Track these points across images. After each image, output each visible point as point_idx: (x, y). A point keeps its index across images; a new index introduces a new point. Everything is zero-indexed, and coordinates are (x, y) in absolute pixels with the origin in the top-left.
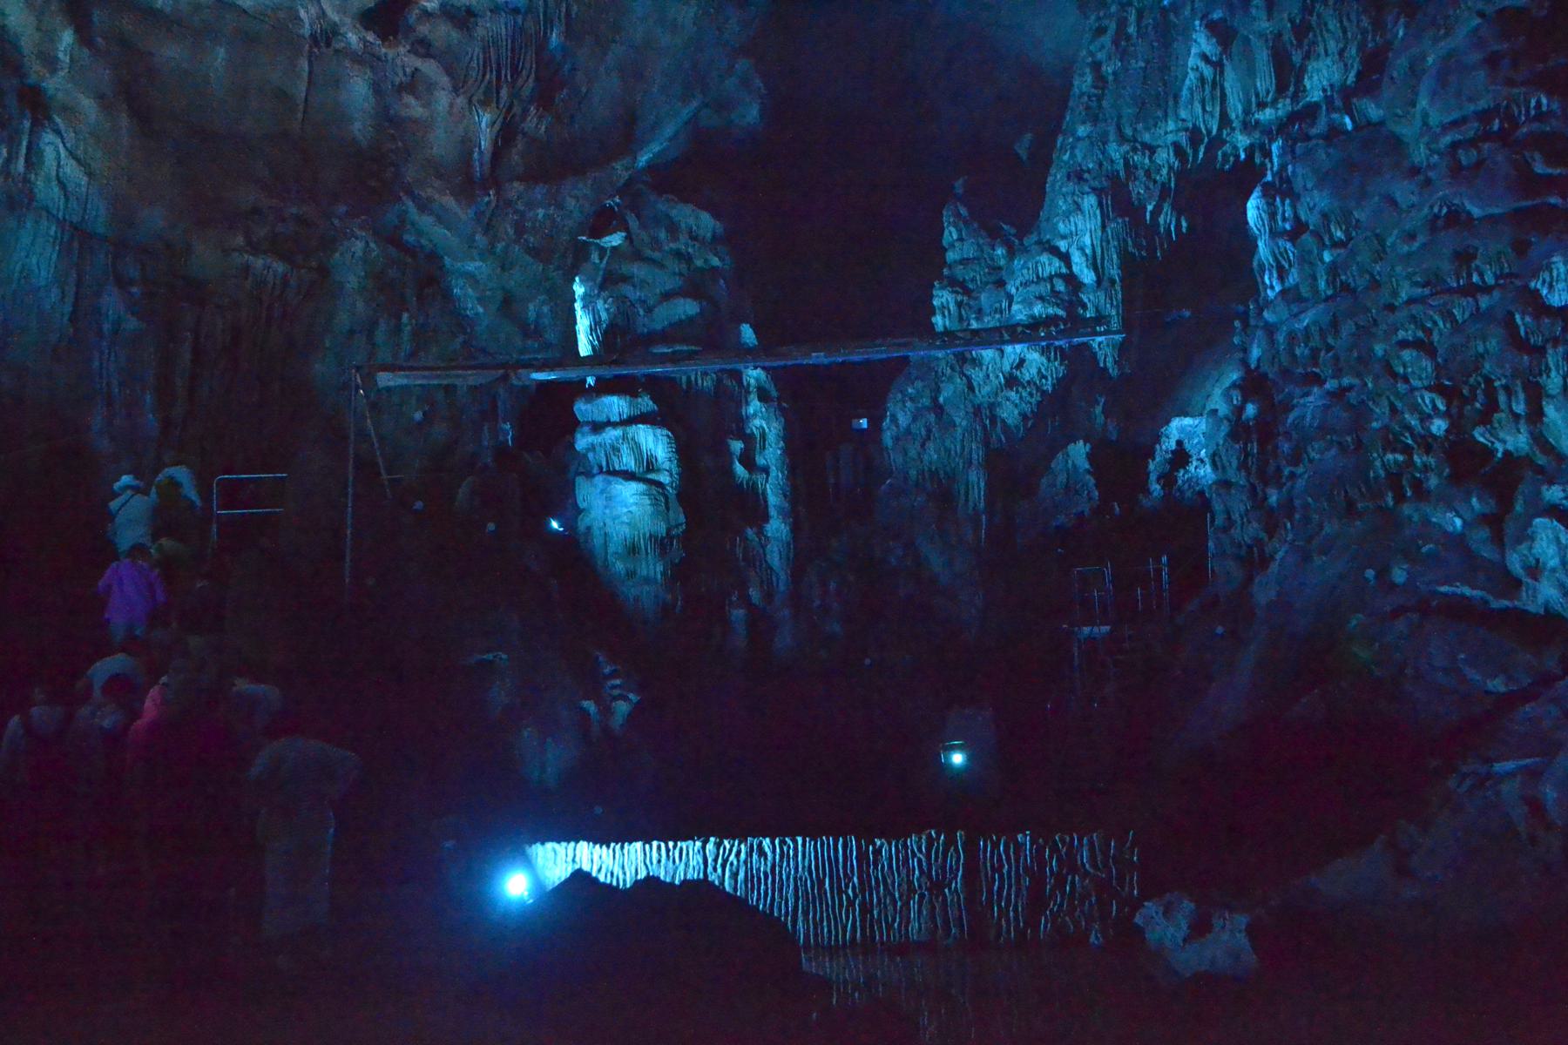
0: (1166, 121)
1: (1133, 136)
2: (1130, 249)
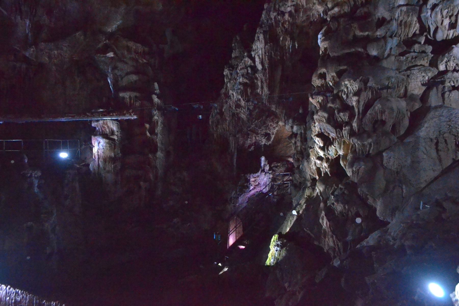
0: (288, 2)
2: (273, 56)
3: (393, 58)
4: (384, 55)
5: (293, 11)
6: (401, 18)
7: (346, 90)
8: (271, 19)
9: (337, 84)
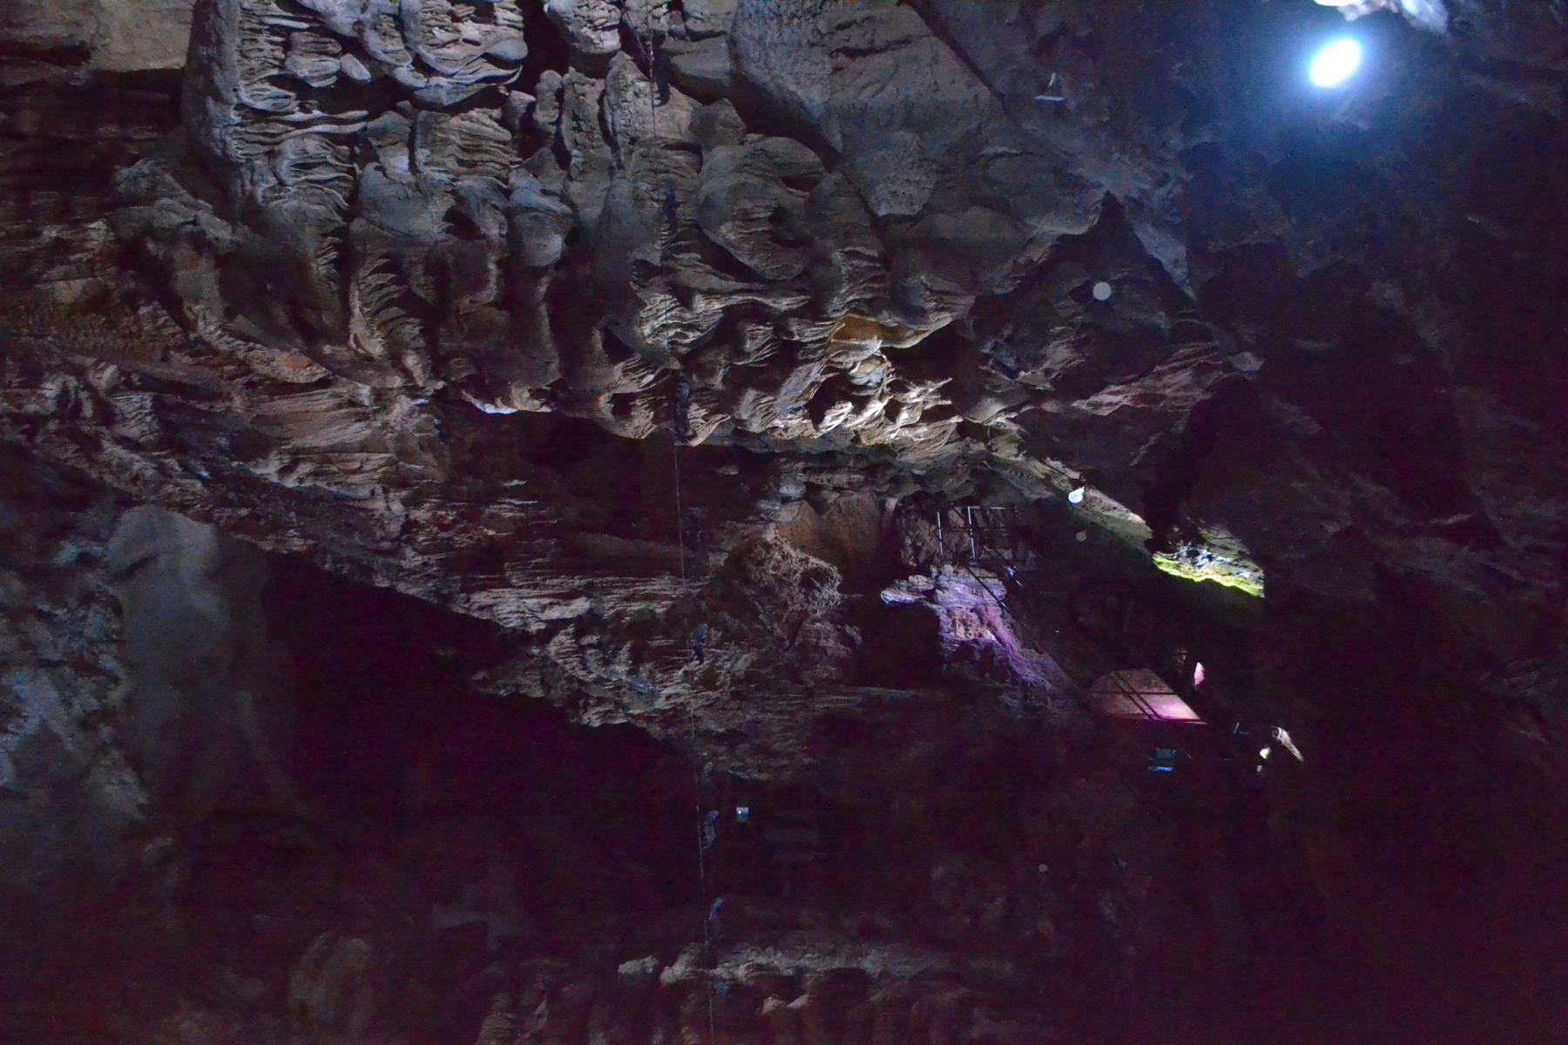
0: (372, 510)
1: (392, 540)
2: (547, 560)
3: (575, 187)
4: (565, 215)
5: (404, 493)
6: (452, 164)
7: (672, 333)
8: (425, 564)
9: (651, 359)
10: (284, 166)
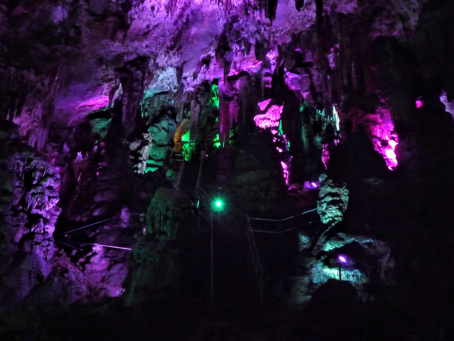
10: (19, 161)
